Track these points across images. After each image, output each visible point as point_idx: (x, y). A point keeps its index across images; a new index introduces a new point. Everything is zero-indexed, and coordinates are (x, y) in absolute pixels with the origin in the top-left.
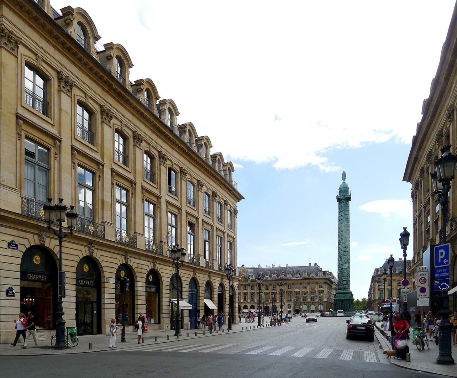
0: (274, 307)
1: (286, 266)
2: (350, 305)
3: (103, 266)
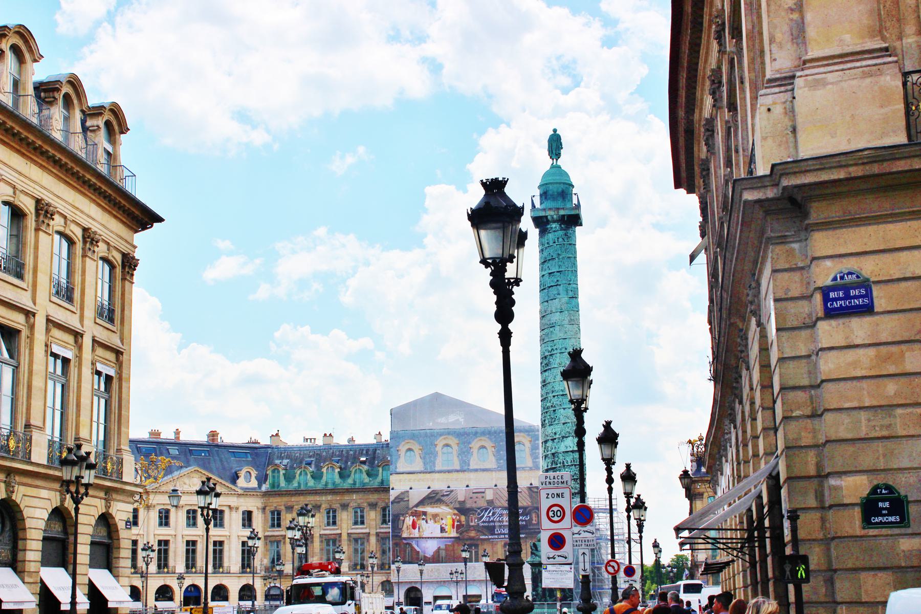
1: (375, 442)
3: (25, 517)
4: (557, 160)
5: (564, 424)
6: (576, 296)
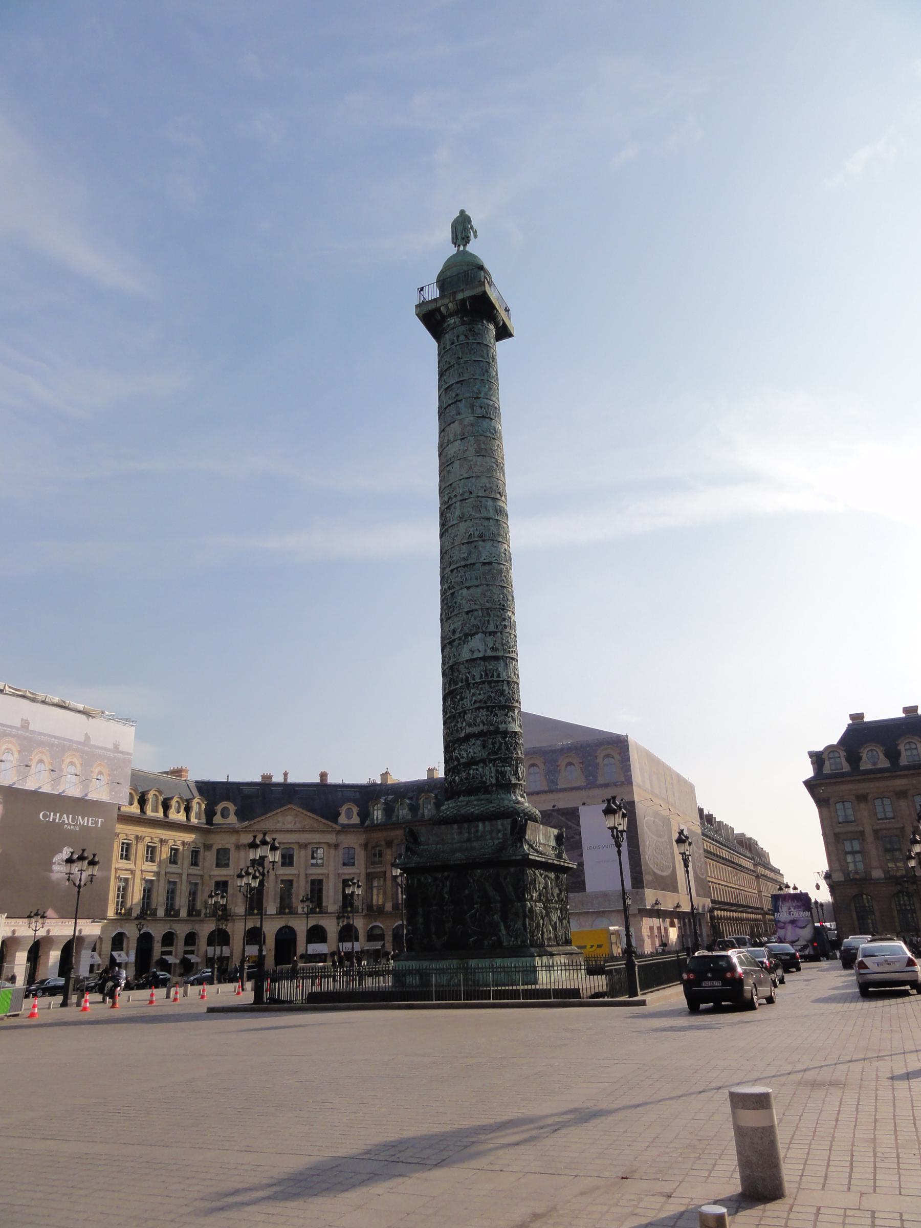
4: (465, 246)
5: (467, 613)
6: (492, 417)
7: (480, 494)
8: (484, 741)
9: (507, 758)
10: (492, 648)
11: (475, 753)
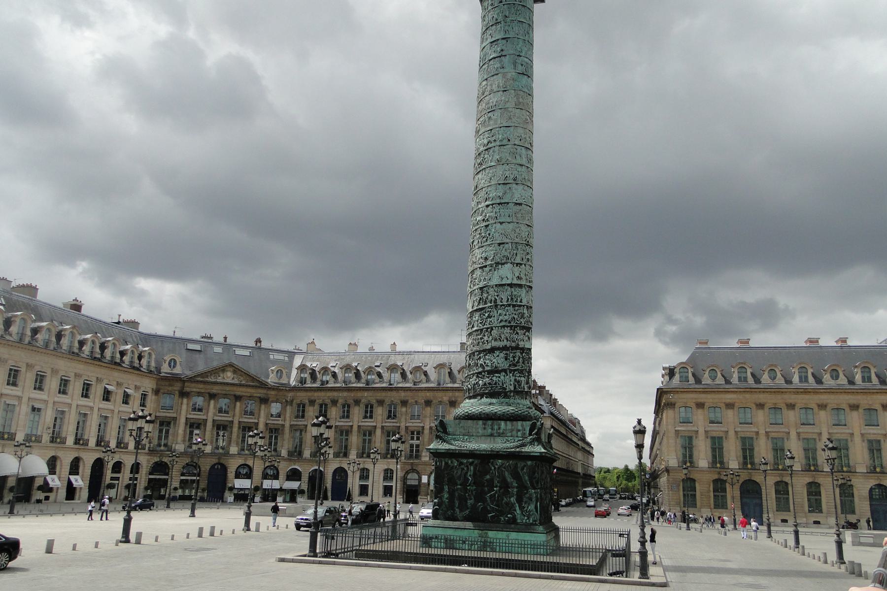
0: (341, 474)
2: (526, 488)
5: (500, 244)
7: (516, 143)
8: (506, 354)
9: (523, 370)
10: (518, 277)
11: (498, 364)
